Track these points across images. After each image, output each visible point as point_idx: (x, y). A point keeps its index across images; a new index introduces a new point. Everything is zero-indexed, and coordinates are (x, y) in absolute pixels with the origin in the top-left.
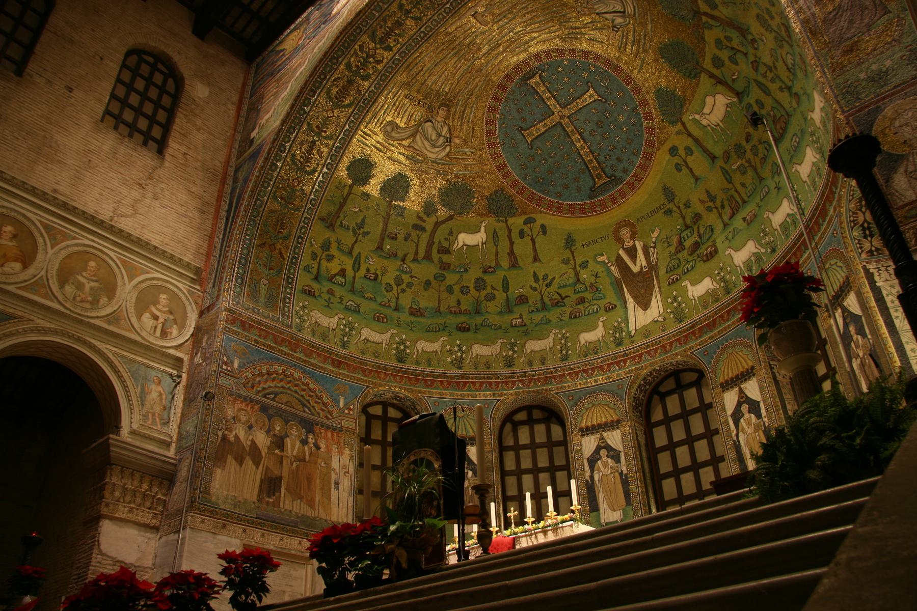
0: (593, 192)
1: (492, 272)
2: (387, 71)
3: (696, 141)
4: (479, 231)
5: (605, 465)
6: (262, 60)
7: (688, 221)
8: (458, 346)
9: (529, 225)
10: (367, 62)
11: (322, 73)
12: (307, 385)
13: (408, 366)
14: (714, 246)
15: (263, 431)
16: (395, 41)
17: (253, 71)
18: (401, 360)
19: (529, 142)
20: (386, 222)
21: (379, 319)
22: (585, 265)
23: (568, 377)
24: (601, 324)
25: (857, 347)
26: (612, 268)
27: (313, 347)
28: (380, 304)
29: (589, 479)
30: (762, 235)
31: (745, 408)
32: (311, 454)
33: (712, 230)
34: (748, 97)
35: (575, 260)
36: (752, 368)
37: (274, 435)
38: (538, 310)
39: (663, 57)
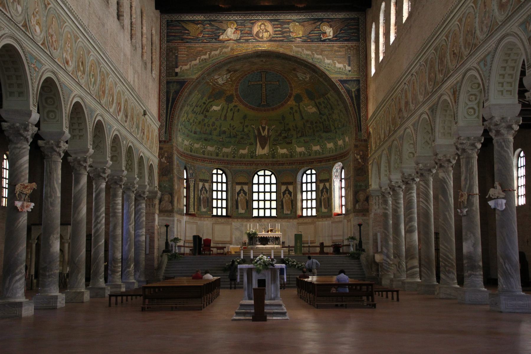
3: (300, 111)
5: (242, 196)
6: (172, 21)
13: (193, 154)
14: (291, 141)
17: (164, 21)
18: (191, 152)
21: (188, 136)
22: (247, 126)
28: (189, 131)
31: (287, 192)
36: (292, 182)
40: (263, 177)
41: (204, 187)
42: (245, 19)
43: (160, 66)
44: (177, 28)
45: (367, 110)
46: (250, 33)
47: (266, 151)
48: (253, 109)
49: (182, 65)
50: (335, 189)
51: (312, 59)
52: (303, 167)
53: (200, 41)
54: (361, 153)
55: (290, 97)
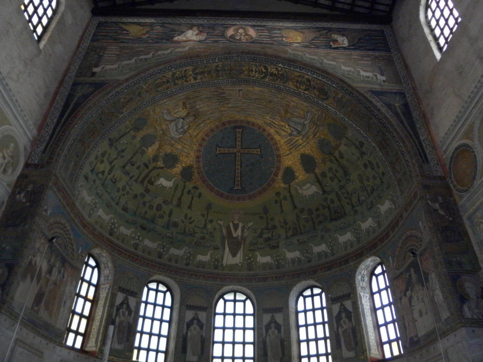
0: (231, 190)
1: (167, 204)
2: (186, 87)
3: (291, 196)
4: (171, 181)
5: (195, 329)
6: (106, 22)
7: (269, 226)
8: (139, 236)
9: (194, 190)
10: (182, 78)
11: (161, 70)
12: (70, 235)
14: (278, 243)
15: (47, 261)
16: (201, 78)
18: (111, 234)
19: (217, 153)
20: (134, 155)
21: (108, 205)
22: (211, 221)
23: (186, 275)
24: (209, 254)
25: (345, 323)
26: (224, 229)
27: (79, 212)
29: (185, 334)
30: (305, 251)
31: (273, 325)
32: (60, 280)
33: (280, 237)
34: (328, 195)
35: (207, 217)
36: (282, 308)
37: (50, 264)
38: (181, 233)
39: (301, 157)
40: (233, 303)
41: (125, 302)
42: (214, 23)
43: (70, 65)
44: (112, 28)
45: (429, 132)
46: (223, 35)
47: (239, 259)
48: (222, 195)
49: (106, 65)
50: (365, 310)
51: (321, 64)
52: (299, 281)
53: (143, 42)
54: (440, 199)
55: (276, 175)
